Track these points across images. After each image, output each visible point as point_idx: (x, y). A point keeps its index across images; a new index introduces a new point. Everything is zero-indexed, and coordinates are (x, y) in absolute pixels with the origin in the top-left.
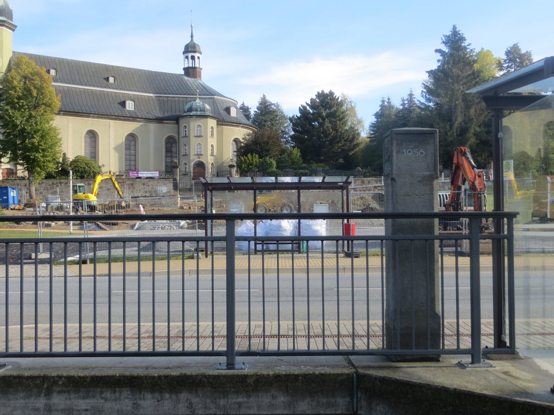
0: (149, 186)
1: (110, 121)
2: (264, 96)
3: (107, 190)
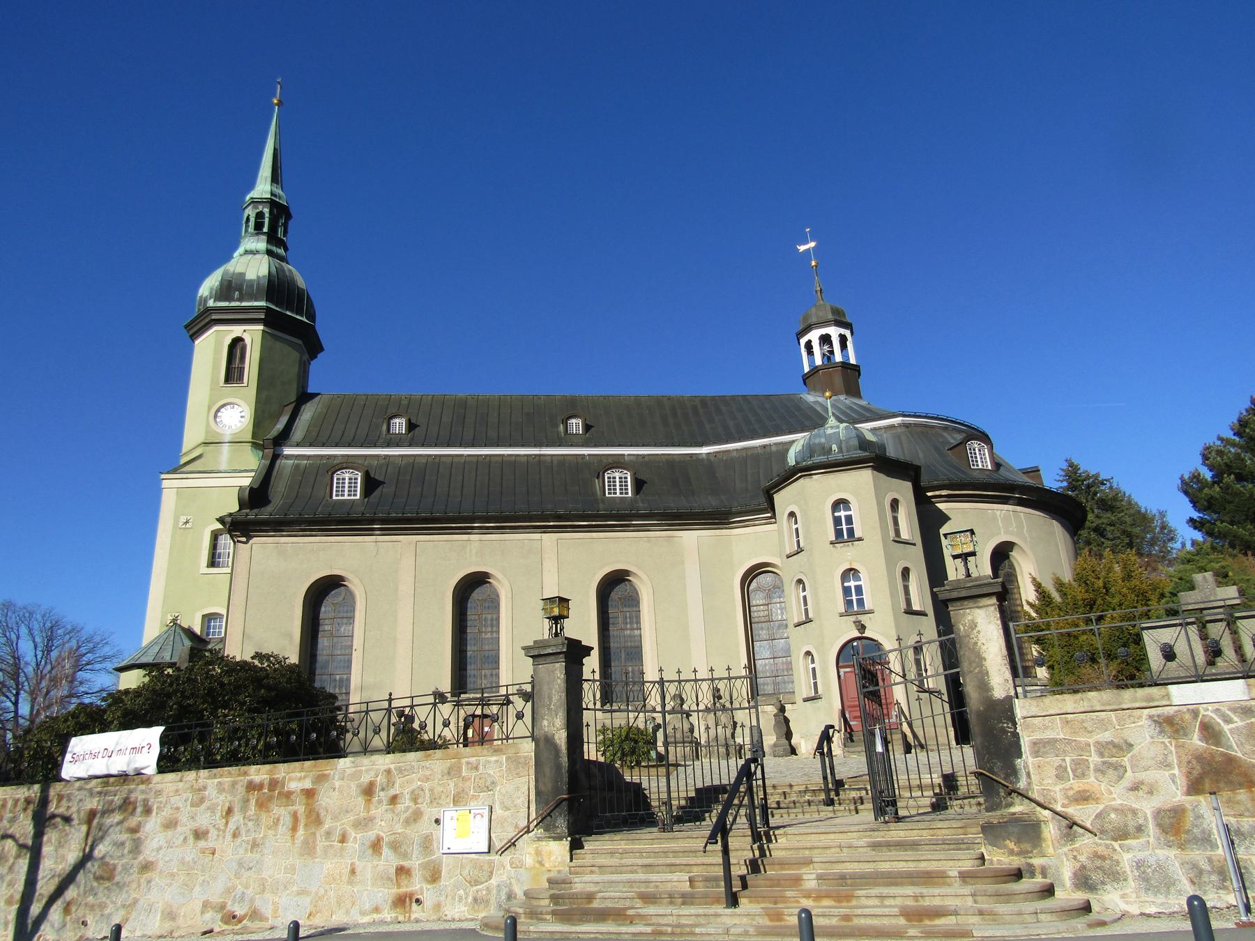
0: (394, 800)
1: (545, 536)
2: (1071, 465)
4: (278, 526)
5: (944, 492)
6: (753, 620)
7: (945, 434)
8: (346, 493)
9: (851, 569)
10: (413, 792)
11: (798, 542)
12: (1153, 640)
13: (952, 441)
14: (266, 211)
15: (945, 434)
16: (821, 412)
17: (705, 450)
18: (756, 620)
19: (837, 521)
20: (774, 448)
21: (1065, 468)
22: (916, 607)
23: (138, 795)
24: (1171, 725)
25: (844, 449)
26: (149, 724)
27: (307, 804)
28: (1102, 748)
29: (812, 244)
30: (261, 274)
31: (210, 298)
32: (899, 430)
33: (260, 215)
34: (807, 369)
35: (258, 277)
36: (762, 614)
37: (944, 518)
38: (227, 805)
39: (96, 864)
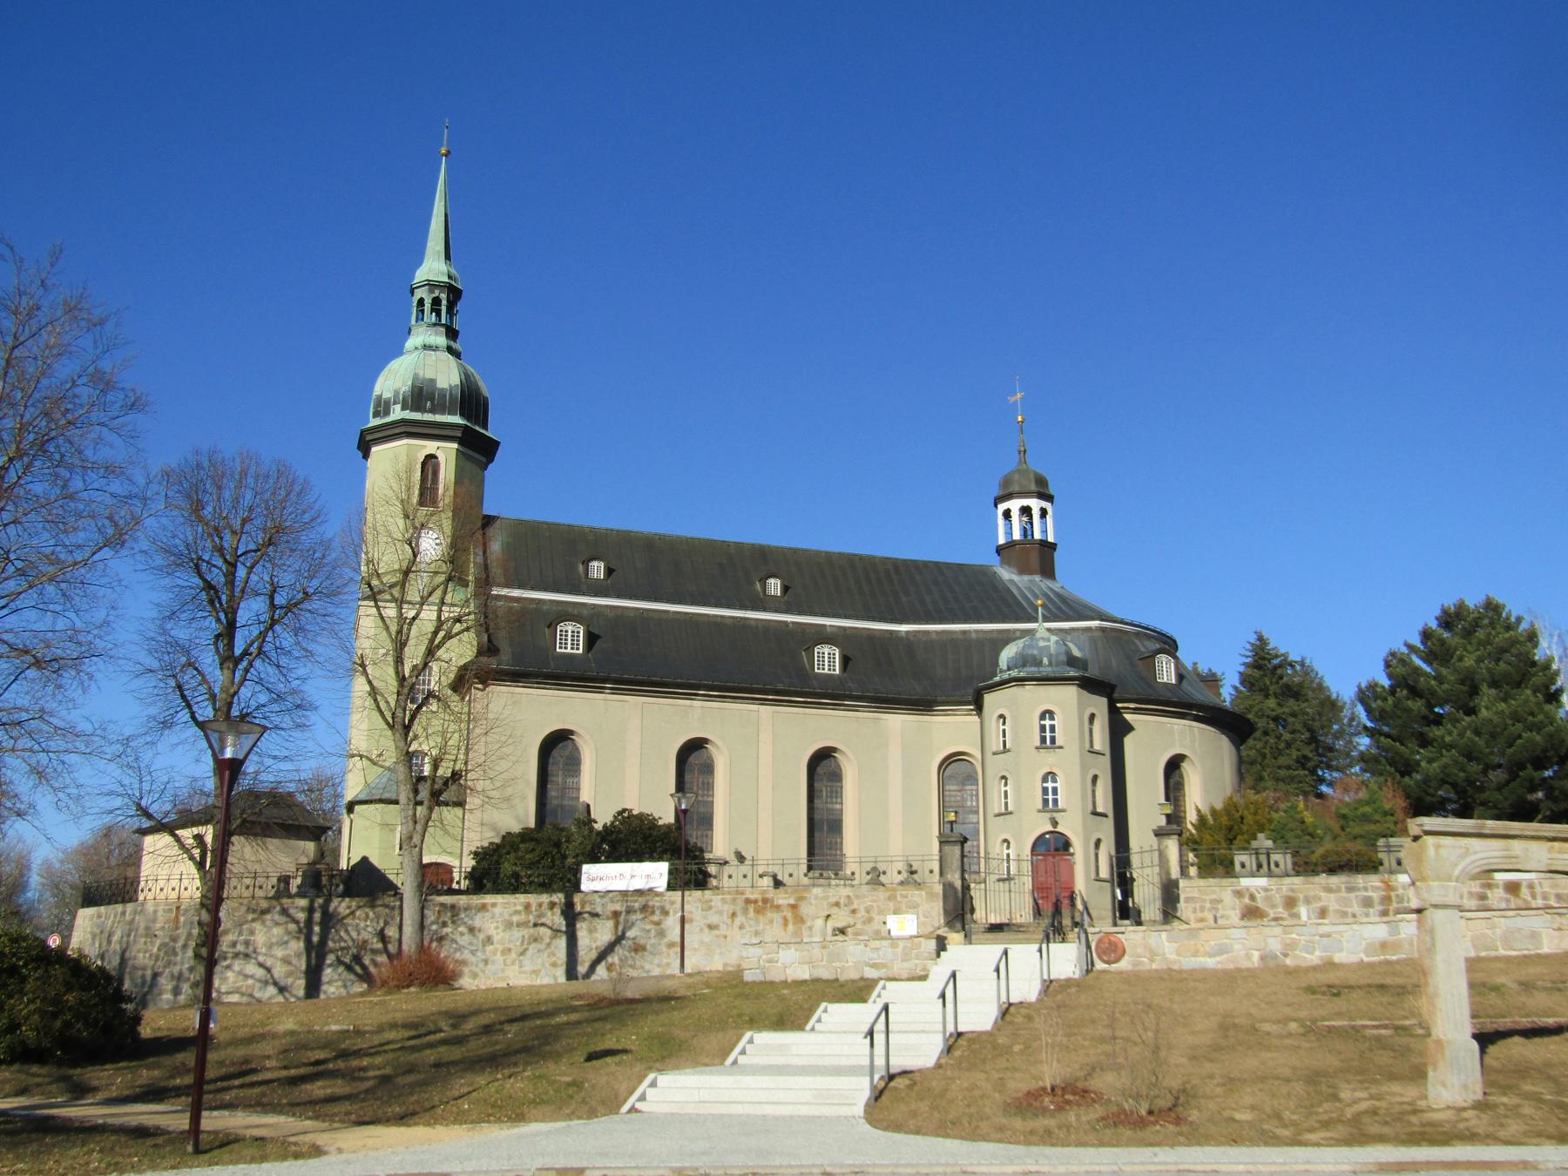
0: (854, 911)
2: (1261, 638)
3: (706, 930)
4: (517, 676)
5: (1132, 705)
6: (946, 804)
7: (1137, 642)
8: (569, 646)
9: (1050, 773)
10: (866, 908)
11: (1004, 742)
12: (1239, 858)
13: (1142, 649)
14: (443, 296)
15: (1137, 642)
16: (1019, 597)
17: (904, 628)
18: (948, 804)
19: (1043, 728)
20: (974, 635)
21: (1253, 641)
22: (1100, 809)
23: (655, 902)
24: (1238, 894)
25: (1054, 663)
26: (654, 858)
27: (793, 913)
28: (1212, 901)
31: (395, 403)
32: (1096, 634)
33: (436, 302)
34: (1002, 541)
35: (450, 386)
36: (953, 799)
37: (1129, 728)
38: (731, 911)
39: (630, 942)
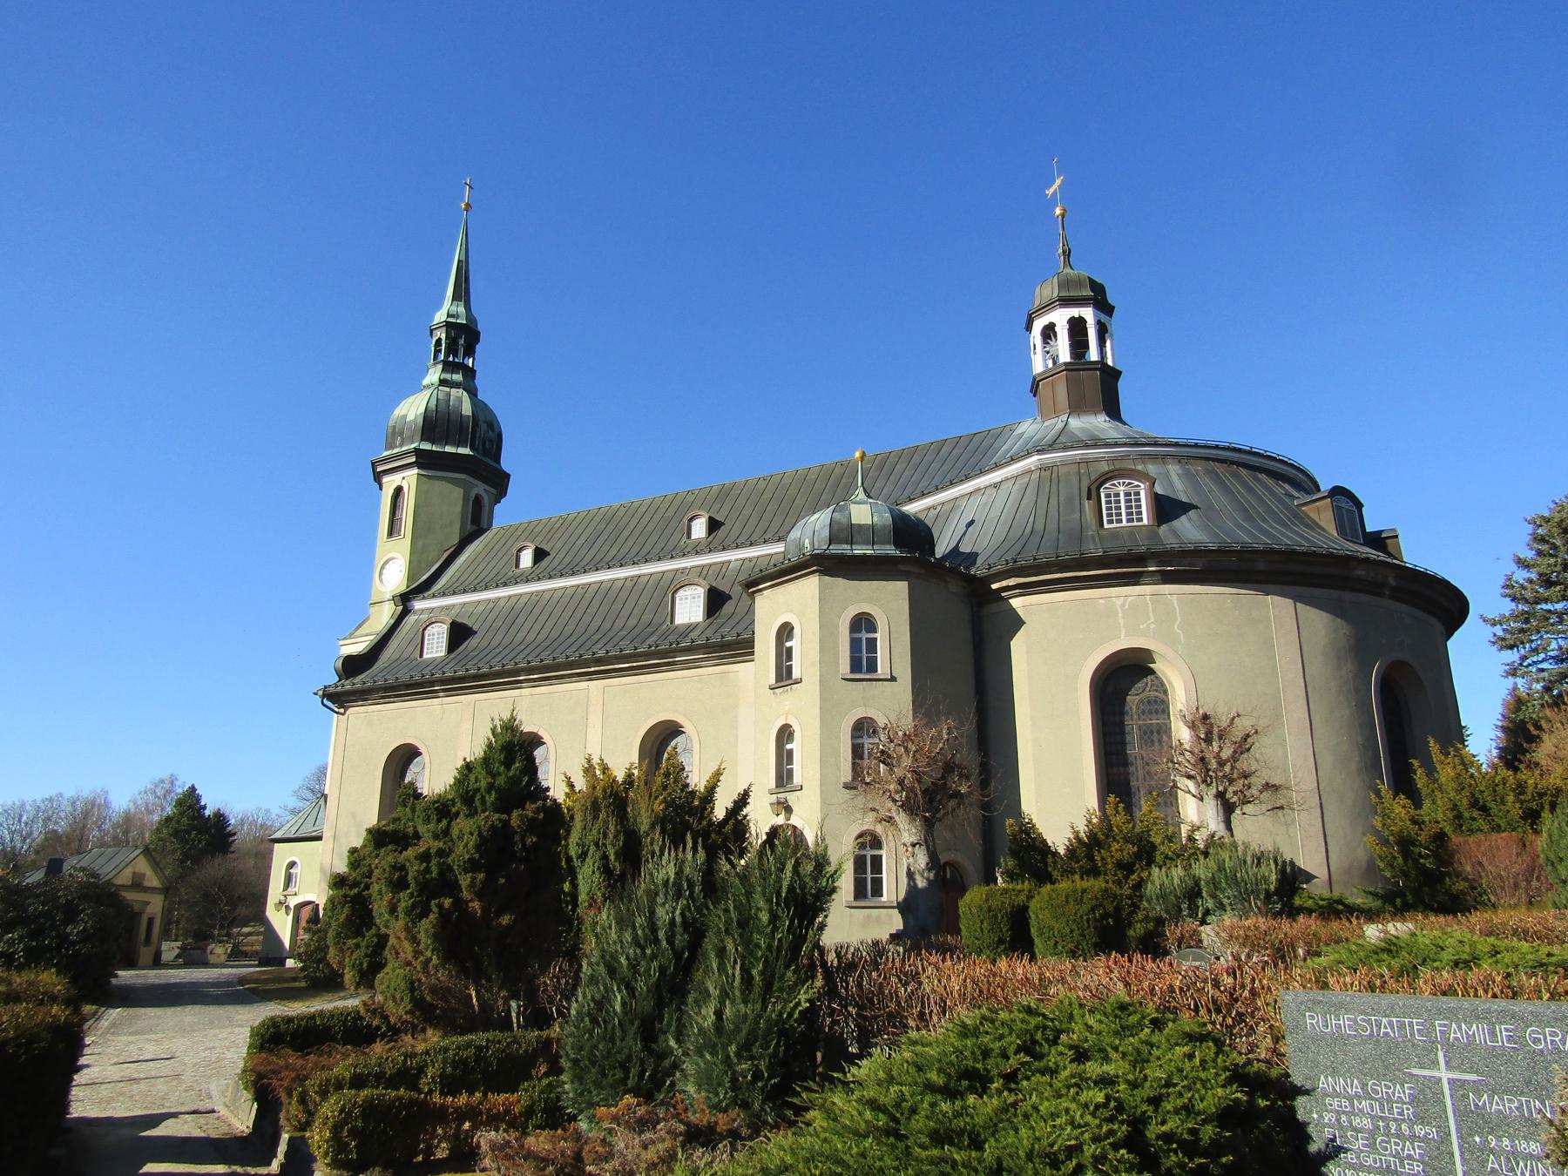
5: (1012, 582)
29: (1058, 182)
30: (418, 414)
